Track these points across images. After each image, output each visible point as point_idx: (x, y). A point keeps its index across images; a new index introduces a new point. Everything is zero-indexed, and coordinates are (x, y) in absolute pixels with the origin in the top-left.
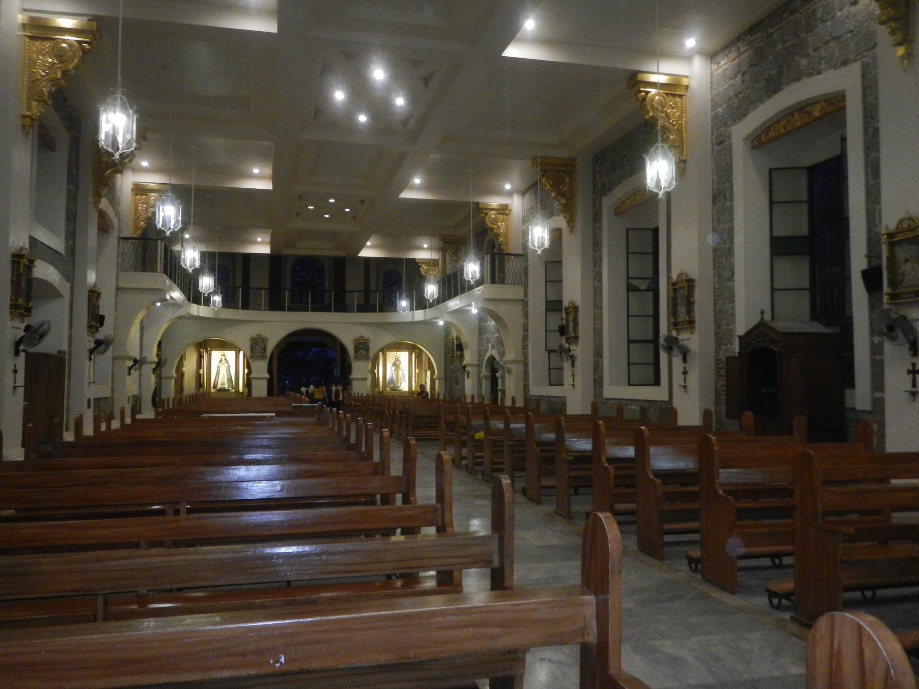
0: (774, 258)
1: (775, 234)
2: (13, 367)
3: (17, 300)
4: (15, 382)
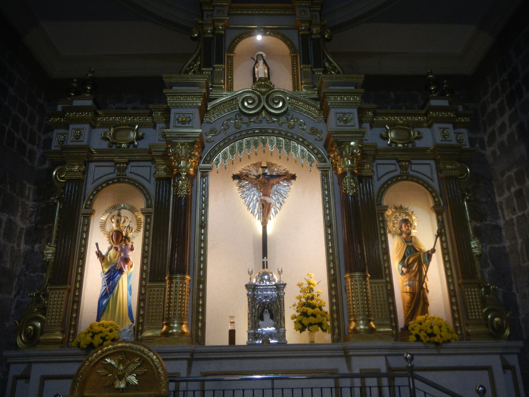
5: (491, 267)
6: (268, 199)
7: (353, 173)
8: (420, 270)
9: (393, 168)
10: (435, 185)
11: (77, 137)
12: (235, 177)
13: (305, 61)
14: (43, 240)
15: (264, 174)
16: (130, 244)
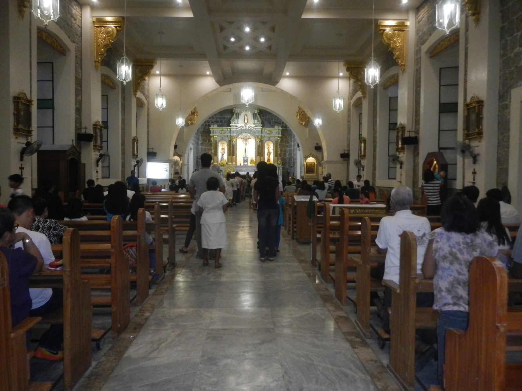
0: (441, 114)
1: (442, 102)
2: (96, 170)
3: (96, 144)
4: (97, 177)
7: (259, 142)
10: (274, 142)
11: (216, 132)
13: (254, 119)
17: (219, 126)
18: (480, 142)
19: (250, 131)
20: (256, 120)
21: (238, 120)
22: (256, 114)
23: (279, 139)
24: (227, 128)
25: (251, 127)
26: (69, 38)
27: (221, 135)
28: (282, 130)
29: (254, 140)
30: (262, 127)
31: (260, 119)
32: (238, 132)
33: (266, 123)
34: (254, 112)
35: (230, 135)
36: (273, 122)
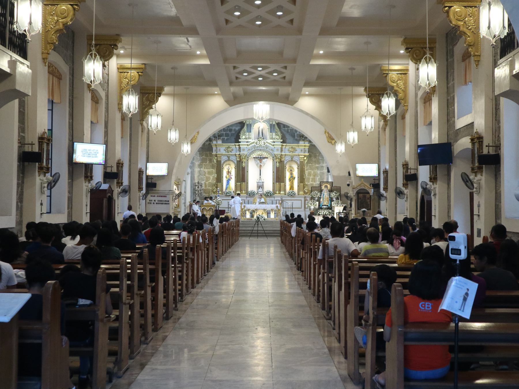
5: (319, 177)
6: (261, 164)
7: (279, 162)
8: (293, 181)
9: (289, 158)
10: (299, 162)
11: (219, 150)
12: (254, 158)
13: (271, 132)
14: (203, 168)
15: (260, 157)
16: (232, 174)
17: (223, 141)
18: (436, 184)
19: (265, 149)
20: (274, 134)
21: (250, 134)
22: (274, 125)
23: (305, 158)
24: (235, 145)
25: (267, 142)
26: (102, 87)
27: (227, 153)
28: (309, 146)
29: (272, 160)
30: (283, 142)
31: (279, 132)
32: (249, 149)
33: (288, 136)
34: (271, 123)
35: (238, 153)
36: (297, 134)
